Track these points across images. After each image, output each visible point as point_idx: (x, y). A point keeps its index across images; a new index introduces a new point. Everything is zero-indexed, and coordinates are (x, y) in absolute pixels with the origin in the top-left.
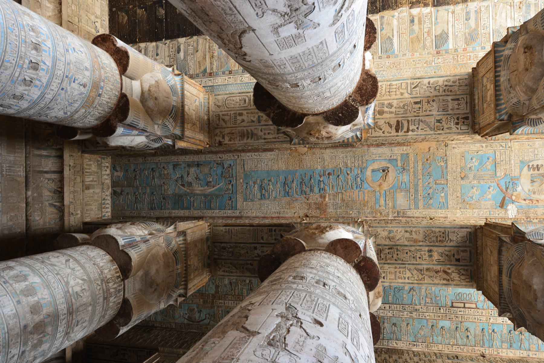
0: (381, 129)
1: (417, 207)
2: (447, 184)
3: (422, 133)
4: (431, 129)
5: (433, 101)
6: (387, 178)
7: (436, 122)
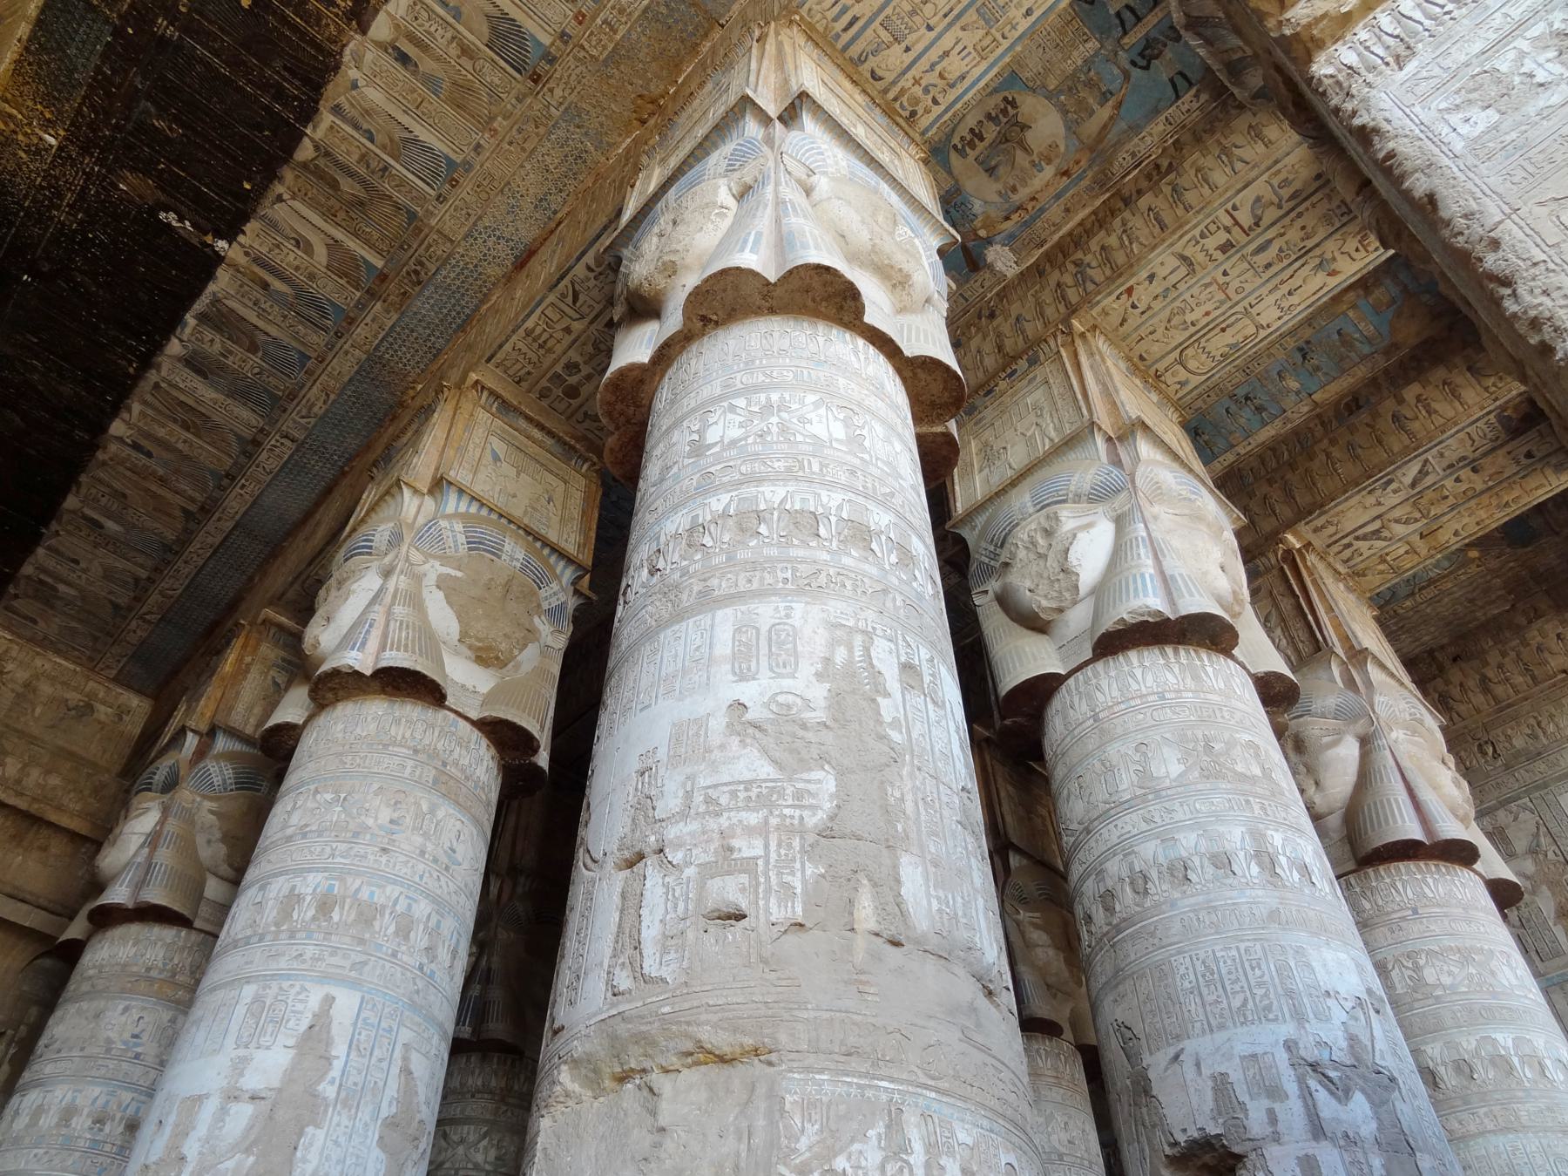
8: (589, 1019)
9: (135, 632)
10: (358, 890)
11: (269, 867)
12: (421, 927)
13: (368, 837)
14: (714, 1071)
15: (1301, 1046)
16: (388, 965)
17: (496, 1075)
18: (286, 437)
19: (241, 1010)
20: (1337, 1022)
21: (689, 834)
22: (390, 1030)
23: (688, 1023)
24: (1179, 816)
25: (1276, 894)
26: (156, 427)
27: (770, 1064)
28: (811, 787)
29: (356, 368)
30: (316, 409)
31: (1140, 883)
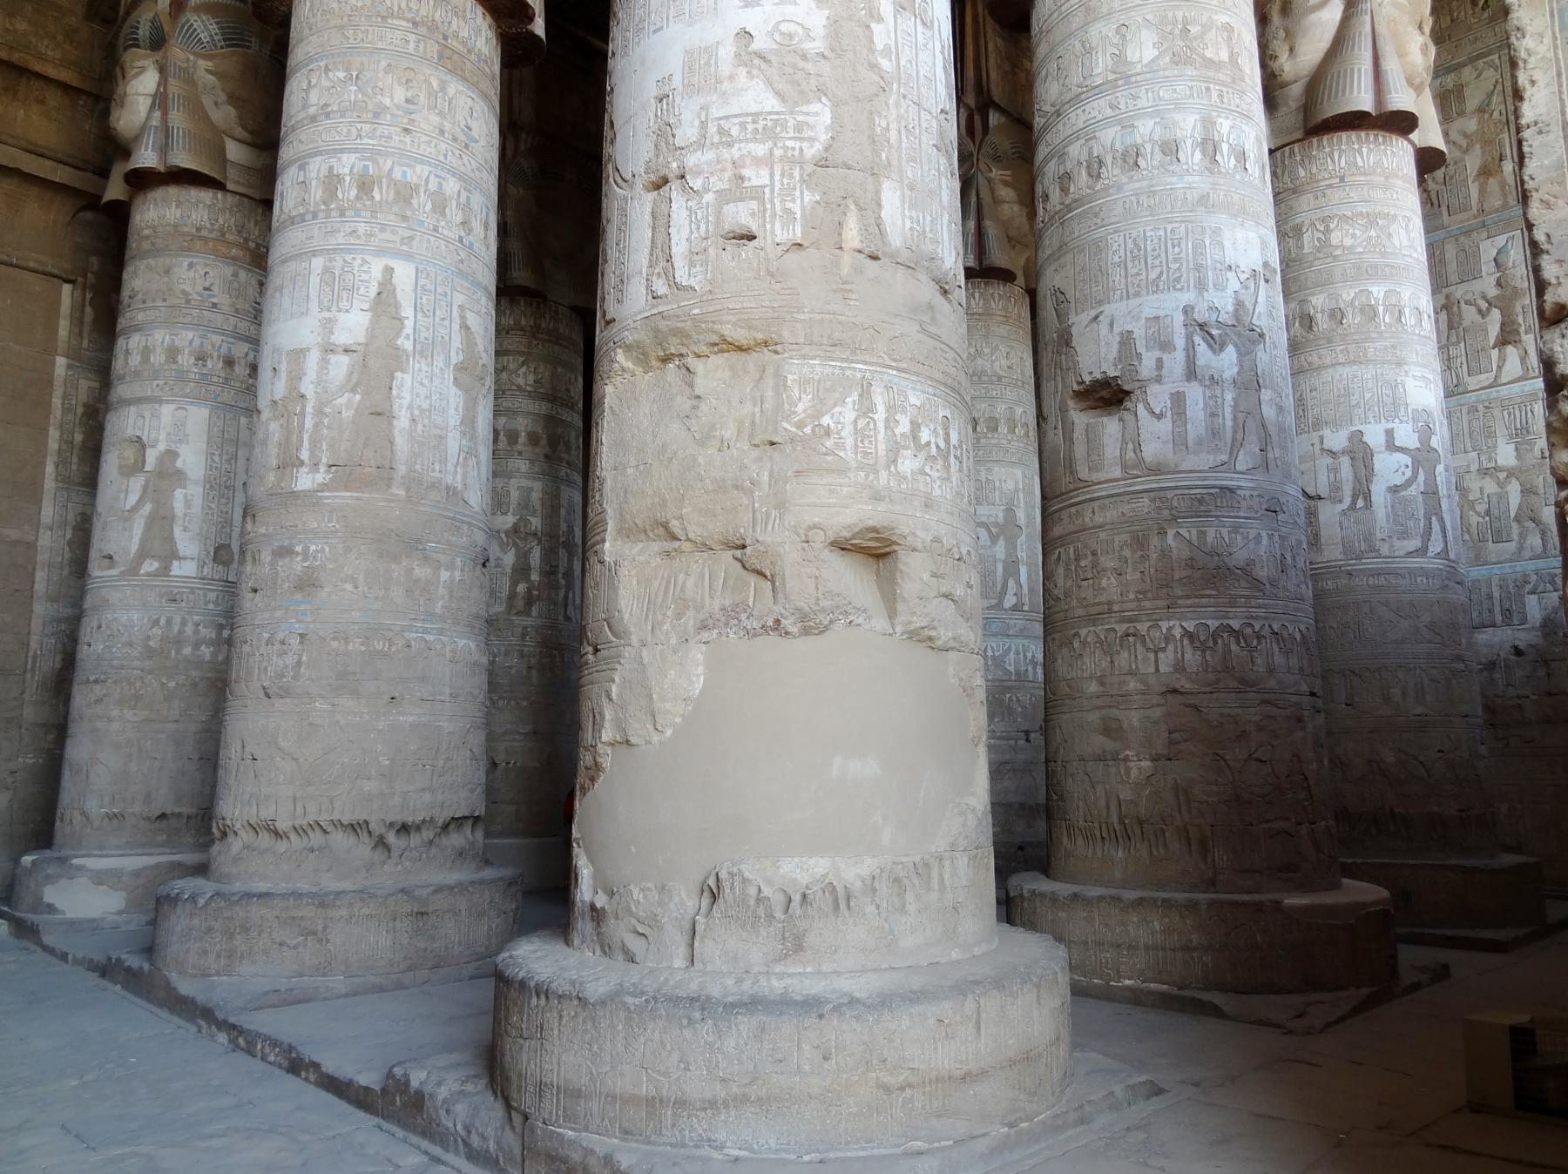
8: (636, 316)
10: (391, 170)
11: (302, 147)
12: (454, 203)
13: (388, 117)
14: (734, 357)
15: (1196, 310)
16: (432, 239)
17: (525, 316)
19: (315, 280)
20: (1230, 291)
21: (706, 162)
22: (446, 295)
23: (714, 322)
24: (1143, 103)
25: (1210, 180)
27: (776, 352)
28: (811, 120)
31: (1095, 167)
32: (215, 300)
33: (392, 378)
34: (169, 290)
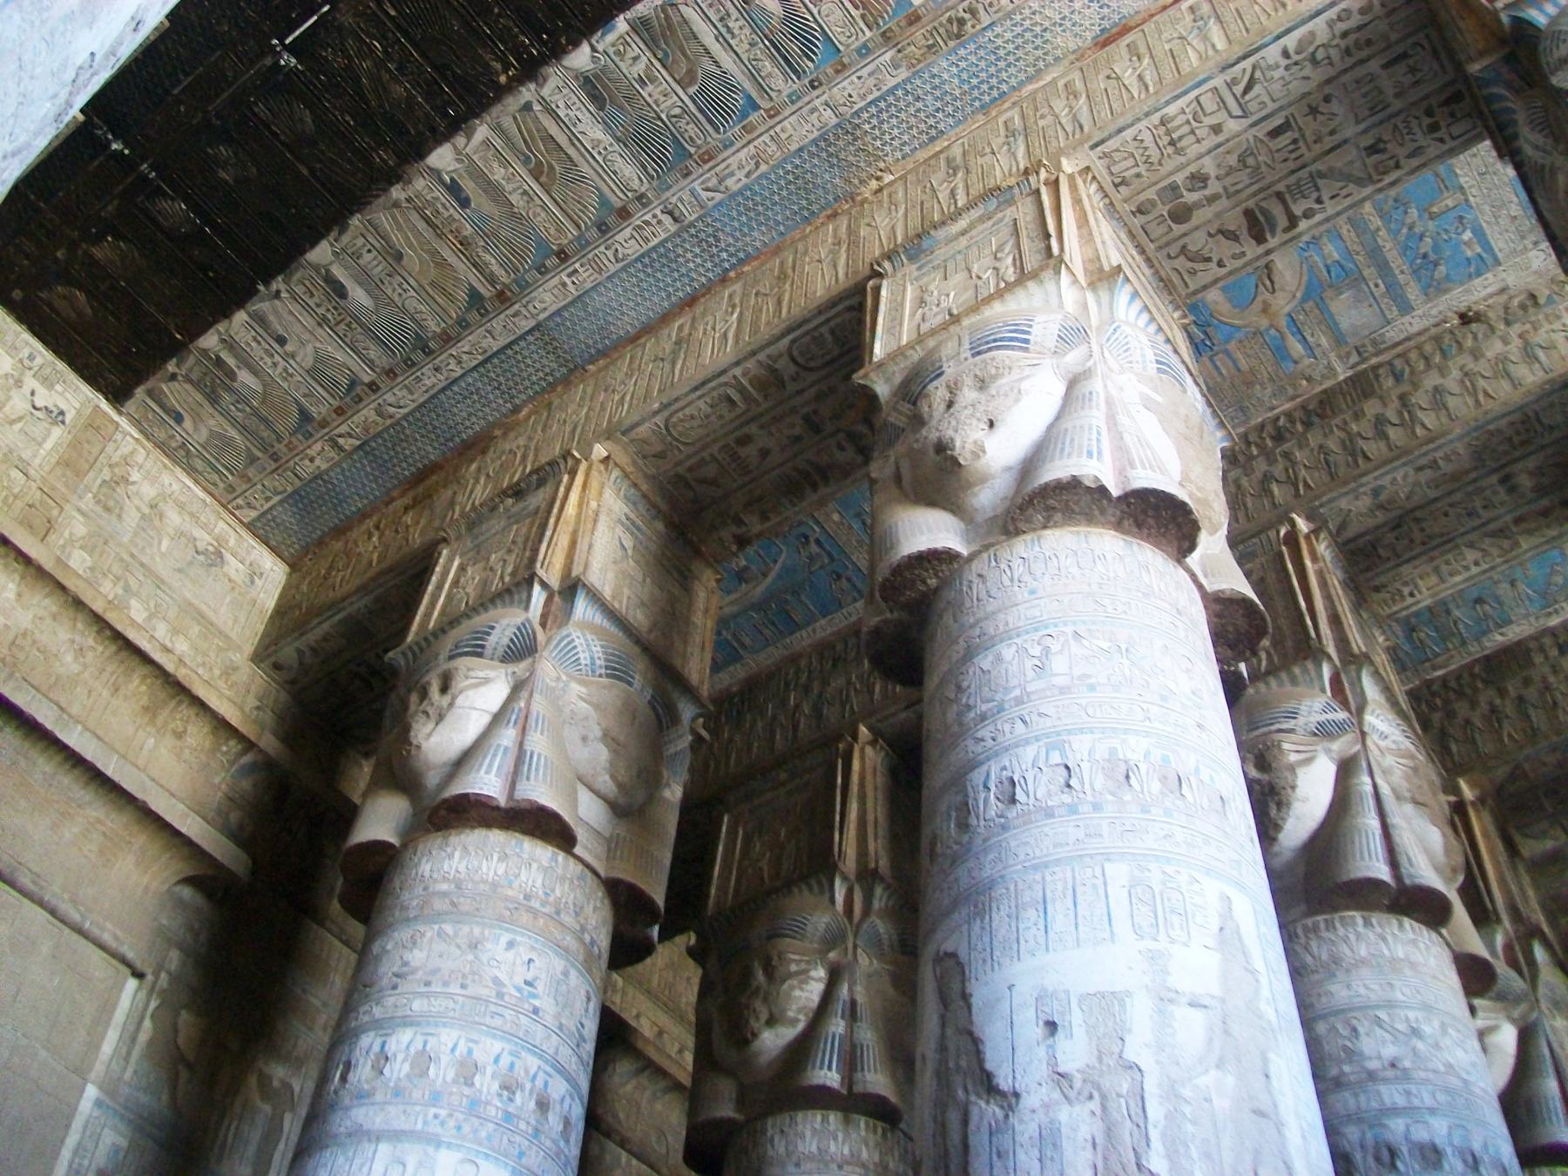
0: (1209, 260)
1: (1406, 308)
2: (1467, 200)
3: (1339, 208)
4: (1360, 182)
5: (1327, 99)
6: (1276, 279)
7: (1369, 155)
9: (312, 460)
18: (670, 213)
26: (495, 165)
29: (816, 134)
30: (730, 182)
32: (537, 1003)
33: (1265, 1060)
34: (474, 973)
